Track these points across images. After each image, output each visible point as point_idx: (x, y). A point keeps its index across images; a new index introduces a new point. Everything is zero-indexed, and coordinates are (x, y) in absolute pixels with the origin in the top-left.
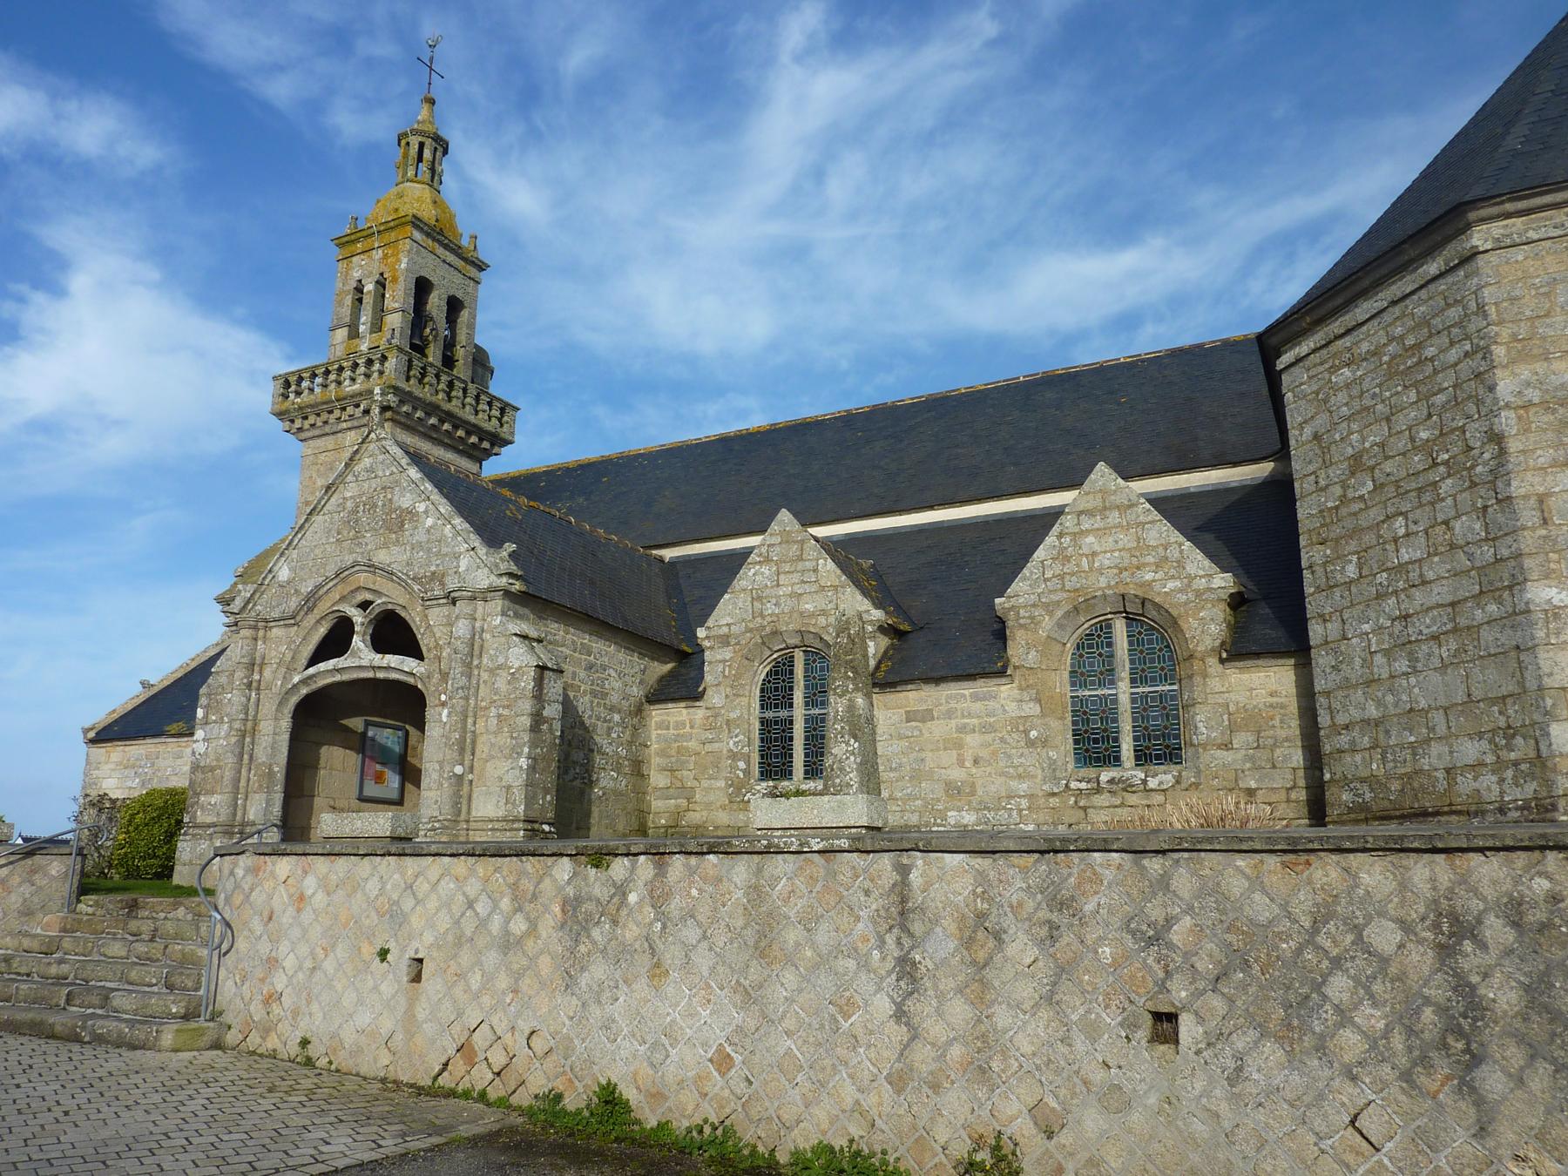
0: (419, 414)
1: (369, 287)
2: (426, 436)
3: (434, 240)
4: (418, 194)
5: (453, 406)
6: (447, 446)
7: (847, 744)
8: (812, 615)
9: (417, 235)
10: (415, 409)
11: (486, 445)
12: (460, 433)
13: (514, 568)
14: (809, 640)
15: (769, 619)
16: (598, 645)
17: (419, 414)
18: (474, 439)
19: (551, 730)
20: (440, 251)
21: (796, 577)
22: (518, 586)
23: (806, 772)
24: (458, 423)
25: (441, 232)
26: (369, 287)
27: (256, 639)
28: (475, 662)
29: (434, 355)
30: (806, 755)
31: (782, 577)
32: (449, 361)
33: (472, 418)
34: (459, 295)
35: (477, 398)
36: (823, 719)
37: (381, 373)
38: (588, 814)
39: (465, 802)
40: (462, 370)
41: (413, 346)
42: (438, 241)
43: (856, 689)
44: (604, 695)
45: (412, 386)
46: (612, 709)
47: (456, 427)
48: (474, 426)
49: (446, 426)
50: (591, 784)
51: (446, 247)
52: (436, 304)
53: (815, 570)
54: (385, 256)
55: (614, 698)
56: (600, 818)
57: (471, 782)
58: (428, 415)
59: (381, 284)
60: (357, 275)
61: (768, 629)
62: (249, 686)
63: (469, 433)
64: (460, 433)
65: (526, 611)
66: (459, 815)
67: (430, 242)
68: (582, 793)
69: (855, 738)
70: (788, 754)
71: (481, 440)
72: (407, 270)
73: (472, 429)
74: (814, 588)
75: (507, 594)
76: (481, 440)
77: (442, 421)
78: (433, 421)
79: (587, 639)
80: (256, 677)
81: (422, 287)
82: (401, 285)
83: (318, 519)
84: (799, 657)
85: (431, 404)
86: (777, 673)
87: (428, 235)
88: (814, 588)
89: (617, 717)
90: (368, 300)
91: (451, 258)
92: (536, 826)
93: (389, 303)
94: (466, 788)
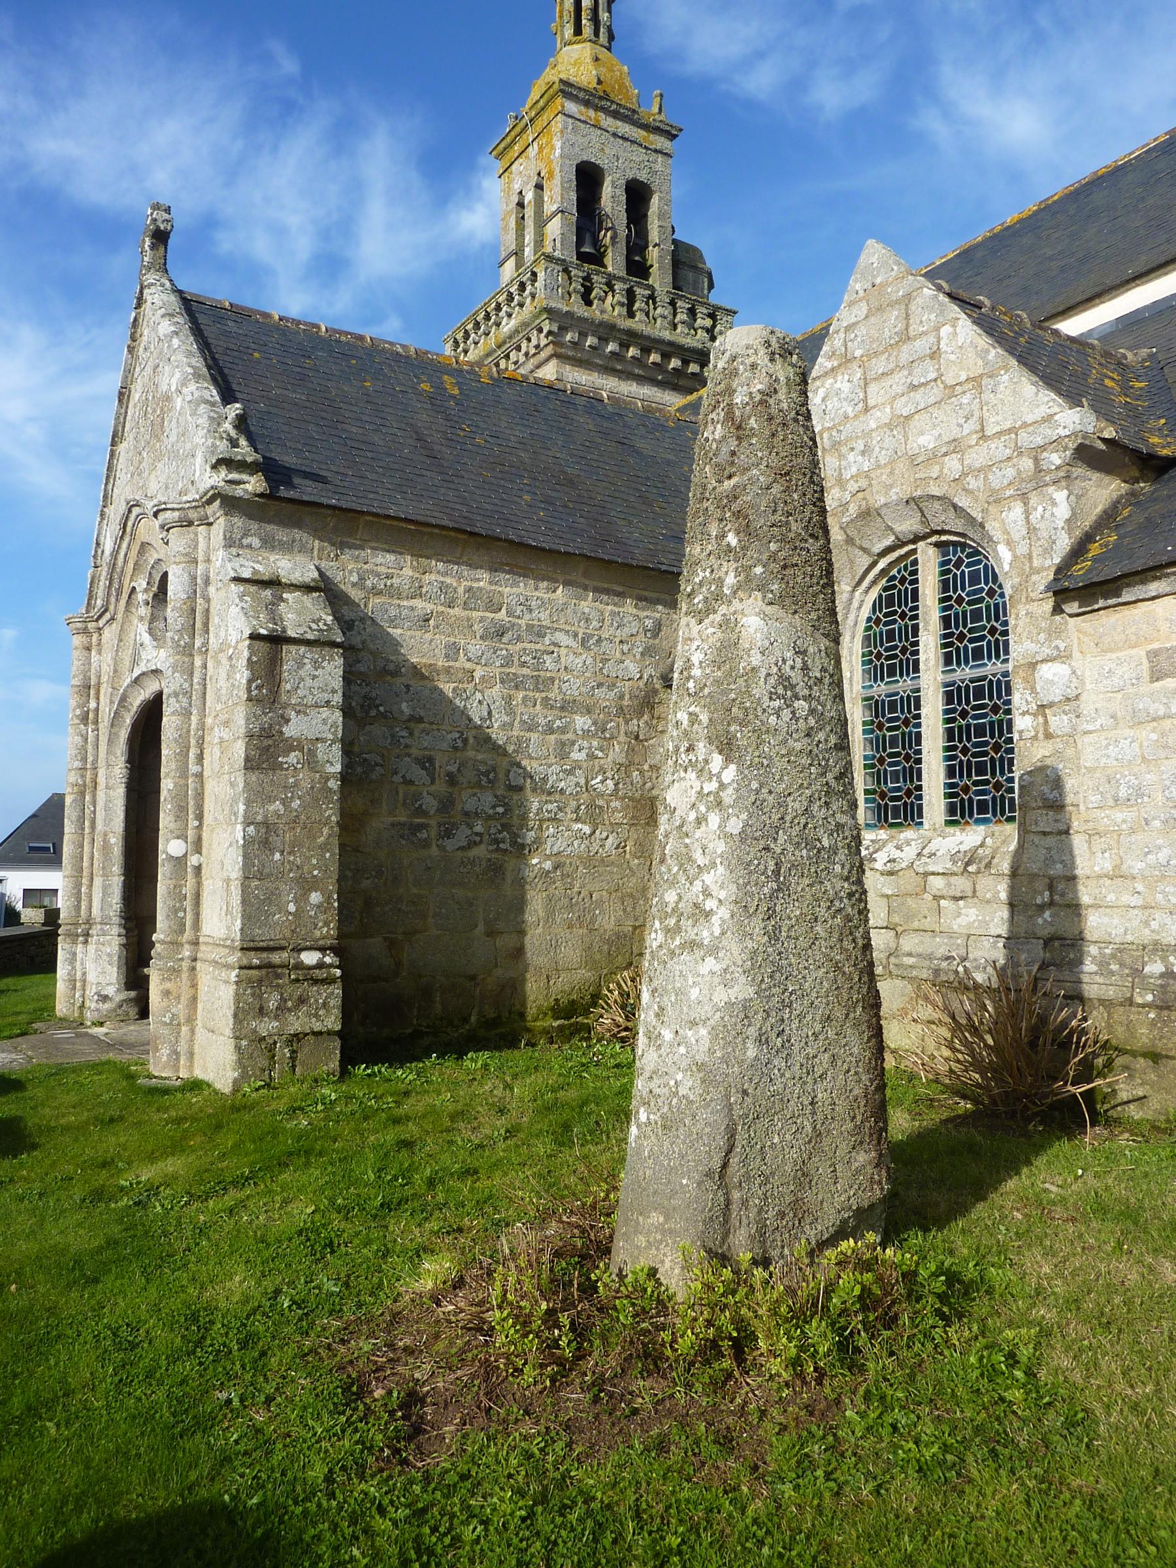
0: (590, 341)
1: (529, 196)
2: (607, 370)
3: (597, 108)
4: (575, 56)
5: (638, 324)
6: (641, 380)
7: (702, 770)
8: (934, 457)
9: (572, 107)
10: (583, 335)
11: (693, 368)
12: (654, 357)
13: (244, 450)
14: (941, 518)
15: (853, 486)
16: (514, 590)
17: (590, 341)
18: (675, 363)
19: (311, 762)
20: (608, 122)
21: (899, 381)
22: (253, 484)
23: (951, 809)
24: (648, 344)
25: (606, 97)
26: (529, 196)
27: (89, 649)
28: (198, 643)
29: (614, 262)
30: (950, 771)
31: (873, 388)
32: (638, 268)
33: (666, 335)
34: (643, 176)
35: (692, 312)
36: (998, 691)
37: (533, 296)
38: (520, 904)
39: (188, 904)
40: (660, 279)
41: (583, 257)
42: (602, 109)
43: (747, 584)
44: (542, 683)
45: (577, 307)
46: (567, 707)
47: (646, 351)
48: (671, 344)
49: (632, 352)
50: (520, 850)
51: (616, 115)
52: (611, 199)
53: (935, 354)
54: (541, 149)
55: (573, 687)
56: (550, 913)
57: (198, 869)
58: (604, 340)
59: (539, 187)
60: (517, 187)
61: (853, 510)
62: (84, 719)
63: (666, 356)
64: (654, 357)
65: (297, 534)
66: (182, 930)
67: (592, 113)
68: (496, 870)
69: (727, 747)
70: (913, 772)
71: (686, 362)
72: (561, 156)
73: (670, 349)
74: (936, 392)
75: (231, 504)
76: (686, 362)
77: (625, 346)
78: (611, 347)
79: (482, 580)
80: (93, 705)
81: (588, 179)
82: (557, 180)
83: (122, 448)
84: (928, 560)
85: (602, 324)
86: (890, 601)
87: (587, 104)
88: (936, 392)
89: (581, 722)
90: (529, 212)
91: (625, 128)
92: (276, 958)
93: (550, 207)
94: (191, 881)
